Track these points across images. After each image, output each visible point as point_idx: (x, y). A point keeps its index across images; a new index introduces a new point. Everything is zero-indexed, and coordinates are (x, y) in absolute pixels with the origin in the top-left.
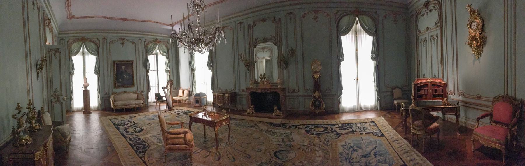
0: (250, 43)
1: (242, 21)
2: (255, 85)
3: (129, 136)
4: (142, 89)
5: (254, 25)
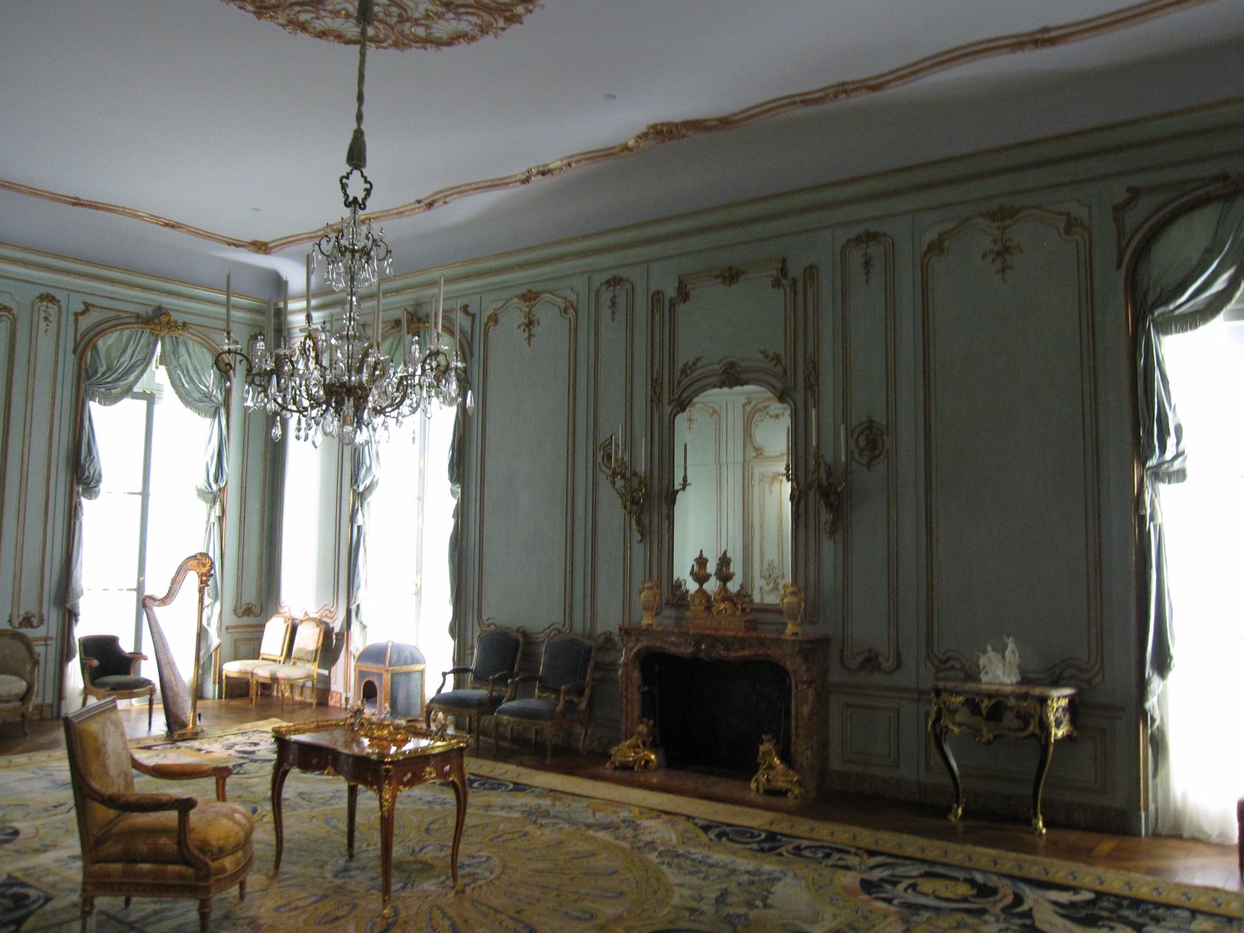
0: (655, 384)
1: (622, 273)
2: (669, 613)
4: (28, 605)
5: (683, 294)
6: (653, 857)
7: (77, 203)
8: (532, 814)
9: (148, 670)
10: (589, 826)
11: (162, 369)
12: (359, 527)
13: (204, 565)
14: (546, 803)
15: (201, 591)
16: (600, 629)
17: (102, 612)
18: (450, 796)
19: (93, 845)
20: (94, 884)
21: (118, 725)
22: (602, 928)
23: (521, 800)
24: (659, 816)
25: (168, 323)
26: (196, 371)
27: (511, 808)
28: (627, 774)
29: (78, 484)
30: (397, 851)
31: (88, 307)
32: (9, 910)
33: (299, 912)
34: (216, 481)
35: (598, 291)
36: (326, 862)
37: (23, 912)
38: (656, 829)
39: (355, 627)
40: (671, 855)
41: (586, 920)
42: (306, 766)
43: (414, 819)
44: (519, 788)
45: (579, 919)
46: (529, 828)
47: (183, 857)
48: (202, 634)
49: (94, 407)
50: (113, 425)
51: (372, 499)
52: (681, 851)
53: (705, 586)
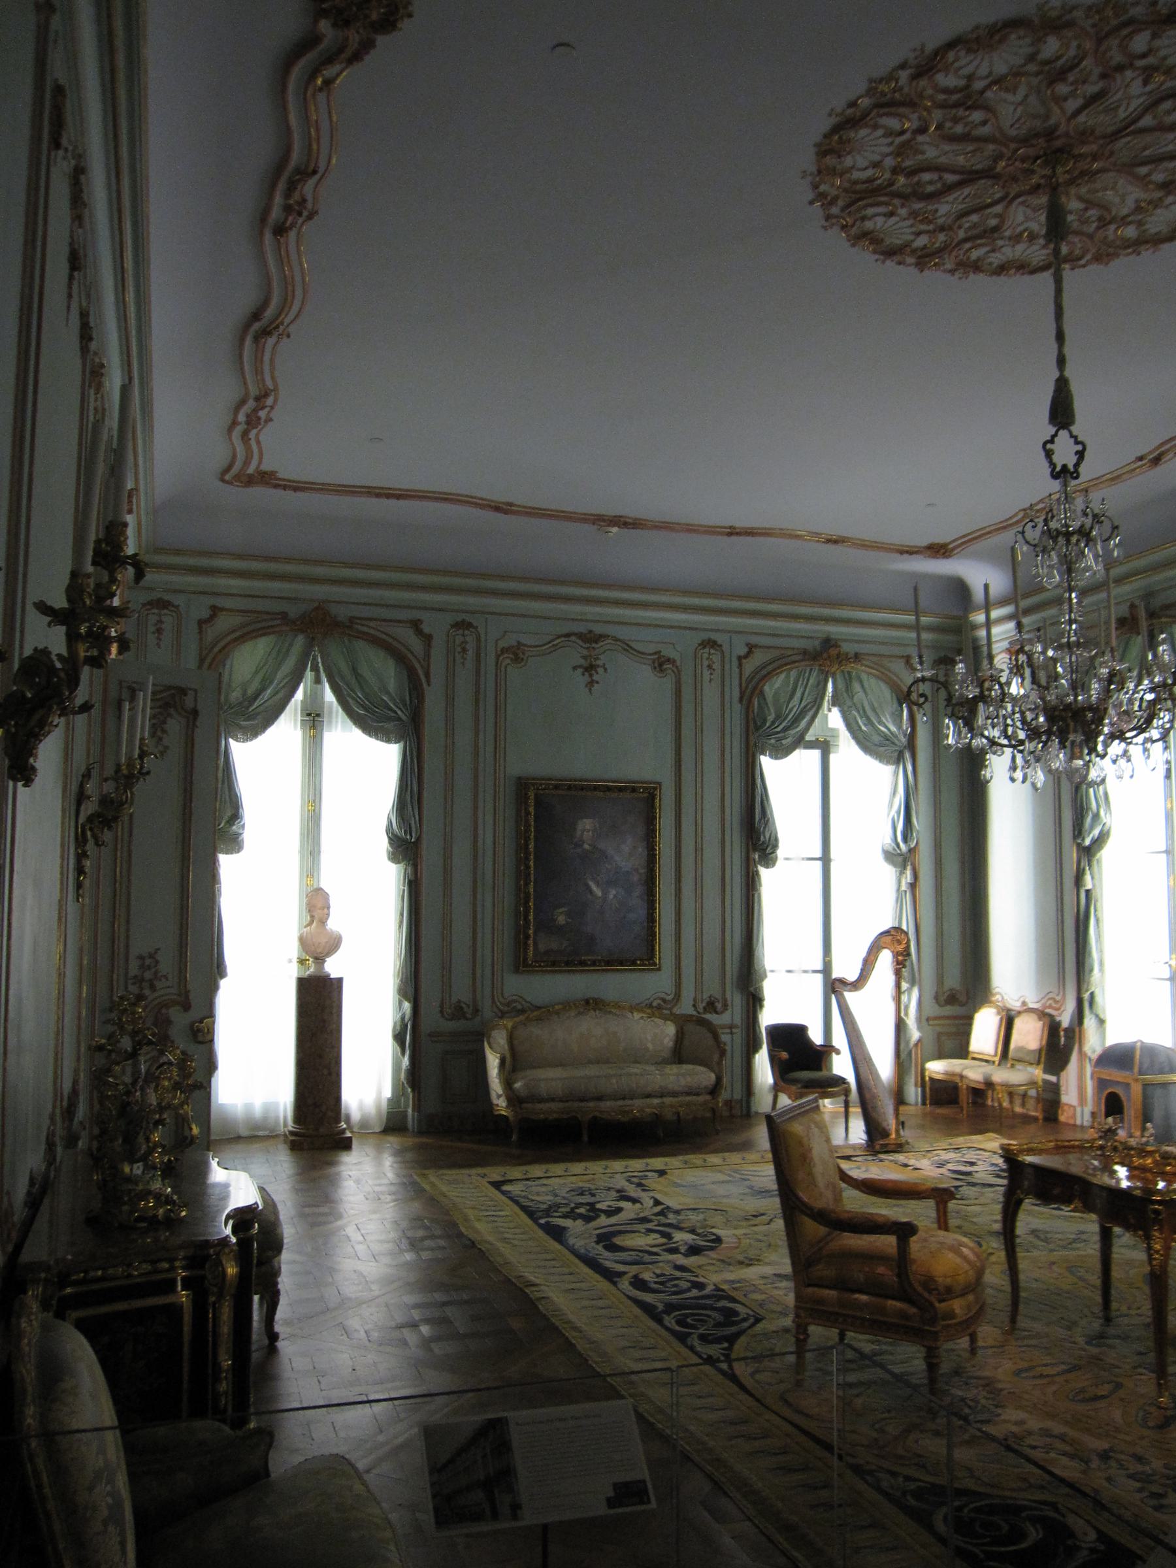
3: (633, 1270)
4: (712, 988)
7: (732, 532)
9: (842, 1066)
12: (1088, 892)
13: (899, 942)
15: (898, 973)
19: (805, 1263)
20: (809, 1310)
25: (838, 656)
26: (874, 710)
29: (755, 850)
31: (751, 648)
32: (718, 1325)
33: (1045, 1381)
34: (905, 839)
36: (1075, 1323)
37: (734, 1329)
39: (1089, 1022)
50: (787, 779)
51: (1106, 855)
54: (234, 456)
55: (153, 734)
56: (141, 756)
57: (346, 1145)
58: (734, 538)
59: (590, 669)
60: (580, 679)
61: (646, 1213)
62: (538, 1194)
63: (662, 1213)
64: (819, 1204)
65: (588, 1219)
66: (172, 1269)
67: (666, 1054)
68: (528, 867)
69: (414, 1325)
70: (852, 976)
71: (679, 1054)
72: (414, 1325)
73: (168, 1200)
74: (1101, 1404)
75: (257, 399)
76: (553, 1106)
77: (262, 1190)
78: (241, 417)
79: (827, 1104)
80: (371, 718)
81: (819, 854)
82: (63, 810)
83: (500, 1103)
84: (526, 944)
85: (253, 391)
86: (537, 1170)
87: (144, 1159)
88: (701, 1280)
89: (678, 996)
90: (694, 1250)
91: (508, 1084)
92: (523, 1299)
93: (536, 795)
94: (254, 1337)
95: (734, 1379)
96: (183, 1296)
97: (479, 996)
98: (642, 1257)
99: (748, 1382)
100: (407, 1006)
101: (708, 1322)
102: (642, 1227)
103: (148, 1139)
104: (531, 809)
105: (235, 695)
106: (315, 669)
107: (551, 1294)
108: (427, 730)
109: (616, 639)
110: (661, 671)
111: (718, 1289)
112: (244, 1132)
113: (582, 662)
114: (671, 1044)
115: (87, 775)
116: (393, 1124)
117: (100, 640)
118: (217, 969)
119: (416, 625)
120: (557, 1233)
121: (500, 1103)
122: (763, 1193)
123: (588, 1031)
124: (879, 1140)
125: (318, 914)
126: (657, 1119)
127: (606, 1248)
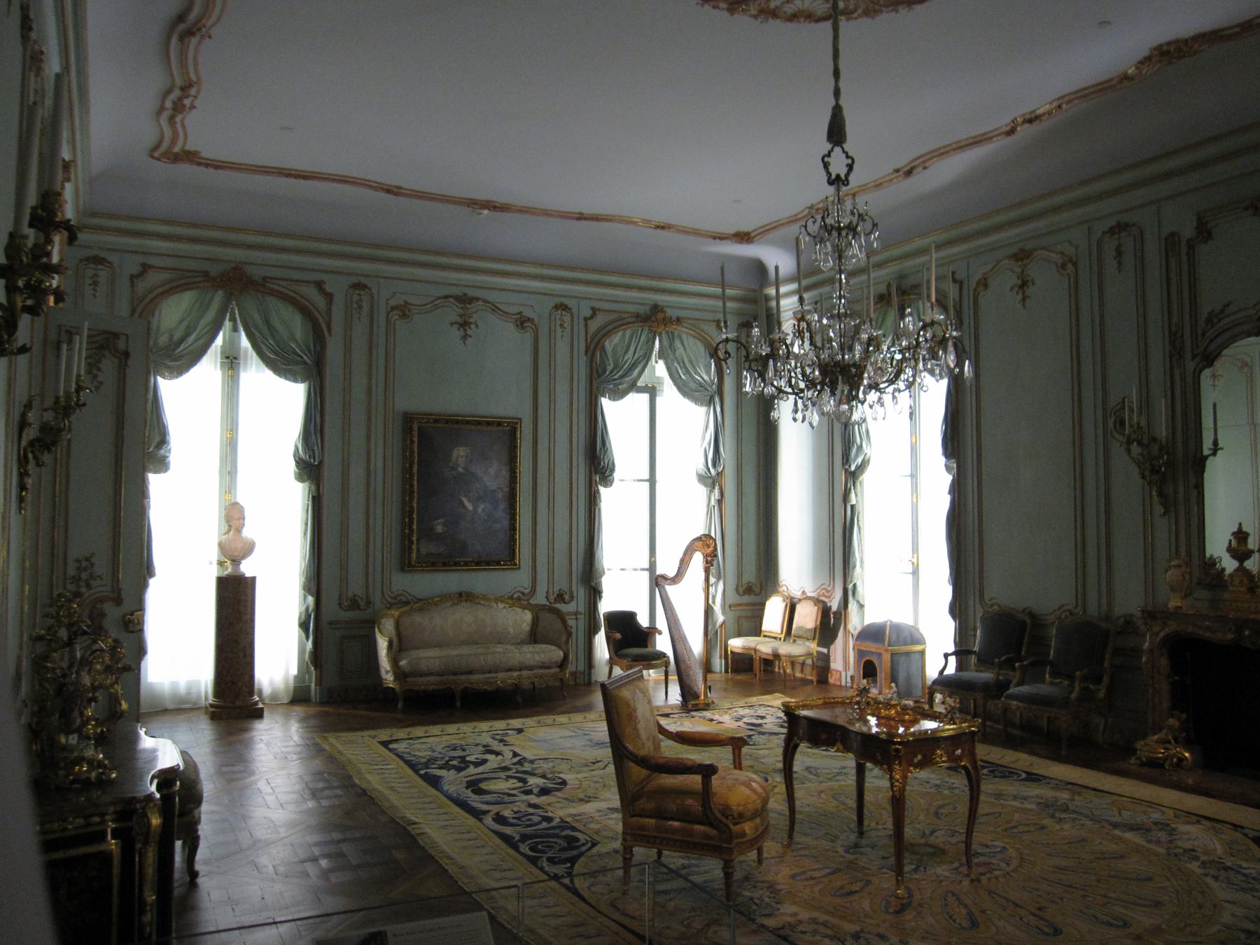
0: (1175, 340)
2: (1203, 594)
4: (561, 583)
6: (1194, 866)
7: (581, 217)
8: (1046, 806)
9: (663, 644)
10: (1115, 826)
11: (661, 362)
12: (852, 506)
13: (708, 546)
14: (1064, 796)
15: (707, 571)
16: (1119, 609)
17: (621, 592)
18: (960, 782)
19: (630, 800)
20: (633, 835)
21: (645, 692)
22: (1138, 938)
23: (1035, 791)
24: (1198, 822)
26: (691, 362)
27: (1025, 798)
28: (1155, 771)
30: (908, 832)
32: (564, 849)
34: (714, 466)
35: (1100, 243)
37: (575, 852)
38: (1193, 835)
39: (852, 606)
40: (1216, 866)
41: (1119, 927)
42: (815, 742)
43: (923, 802)
44: (1032, 778)
45: (1109, 924)
46: (1046, 821)
47: (707, 818)
48: (708, 611)
49: (605, 402)
50: (622, 417)
51: (867, 478)
52: (1229, 864)
53: (1248, 564)
54: (162, 136)
55: (89, 372)
56: (79, 389)
57: (259, 715)
58: (583, 222)
59: (464, 325)
60: (457, 333)
61: (507, 763)
62: (419, 750)
63: (519, 763)
64: (642, 753)
65: (459, 769)
66: (103, 822)
67: (523, 636)
68: (412, 486)
69: (314, 860)
70: (671, 573)
71: (535, 636)
72: (314, 860)
73: (100, 764)
74: (856, 897)
75: (182, 89)
76: (432, 679)
77: (184, 754)
78: (169, 104)
79: (652, 675)
80: (281, 361)
81: (647, 477)
82: (7, 437)
83: (388, 678)
84: (410, 549)
85: (179, 82)
86: (419, 731)
87: (78, 730)
88: (550, 814)
89: (533, 590)
90: (544, 791)
91: (394, 662)
92: (405, 836)
93: (420, 429)
94: (177, 875)
95: (576, 893)
96: (113, 844)
97: (371, 590)
98: (504, 798)
99: (586, 894)
100: (311, 599)
101: (555, 847)
102: (503, 775)
103: (82, 714)
104: (416, 439)
105: (163, 340)
106: (233, 319)
107: (428, 830)
108: (328, 371)
109: (486, 301)
110: (524, 328)
111: (562, 821)
112: (170, 706)
113: (459, 320)
114: (528, 628)
115: (28, 406)
116: (299, 697)
117: (38, 292)
118: (145, 570)
119: (319, 285)
120: (434, 782)
121: (388, 678)
122: (599, 744)
123: (461, 618)
124: (690, 701)
125: (235, 523)
126: (517, 689)
127: (474, 792)
